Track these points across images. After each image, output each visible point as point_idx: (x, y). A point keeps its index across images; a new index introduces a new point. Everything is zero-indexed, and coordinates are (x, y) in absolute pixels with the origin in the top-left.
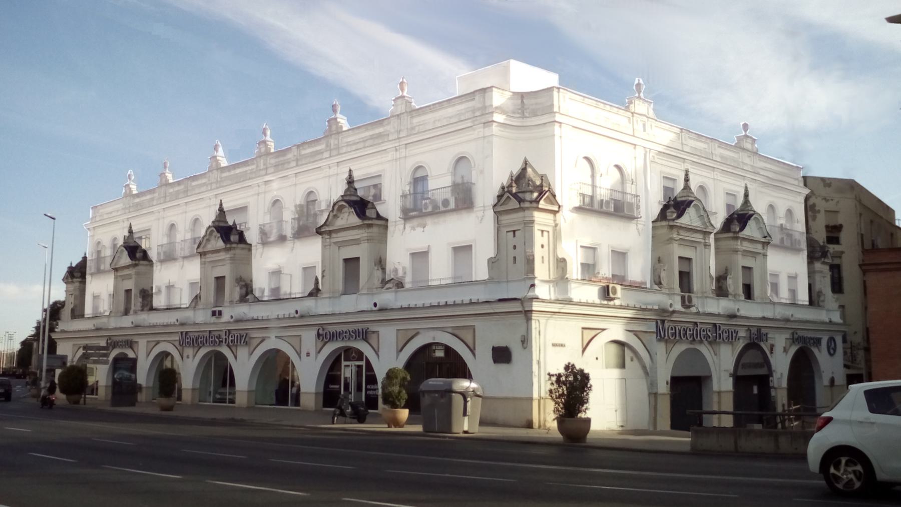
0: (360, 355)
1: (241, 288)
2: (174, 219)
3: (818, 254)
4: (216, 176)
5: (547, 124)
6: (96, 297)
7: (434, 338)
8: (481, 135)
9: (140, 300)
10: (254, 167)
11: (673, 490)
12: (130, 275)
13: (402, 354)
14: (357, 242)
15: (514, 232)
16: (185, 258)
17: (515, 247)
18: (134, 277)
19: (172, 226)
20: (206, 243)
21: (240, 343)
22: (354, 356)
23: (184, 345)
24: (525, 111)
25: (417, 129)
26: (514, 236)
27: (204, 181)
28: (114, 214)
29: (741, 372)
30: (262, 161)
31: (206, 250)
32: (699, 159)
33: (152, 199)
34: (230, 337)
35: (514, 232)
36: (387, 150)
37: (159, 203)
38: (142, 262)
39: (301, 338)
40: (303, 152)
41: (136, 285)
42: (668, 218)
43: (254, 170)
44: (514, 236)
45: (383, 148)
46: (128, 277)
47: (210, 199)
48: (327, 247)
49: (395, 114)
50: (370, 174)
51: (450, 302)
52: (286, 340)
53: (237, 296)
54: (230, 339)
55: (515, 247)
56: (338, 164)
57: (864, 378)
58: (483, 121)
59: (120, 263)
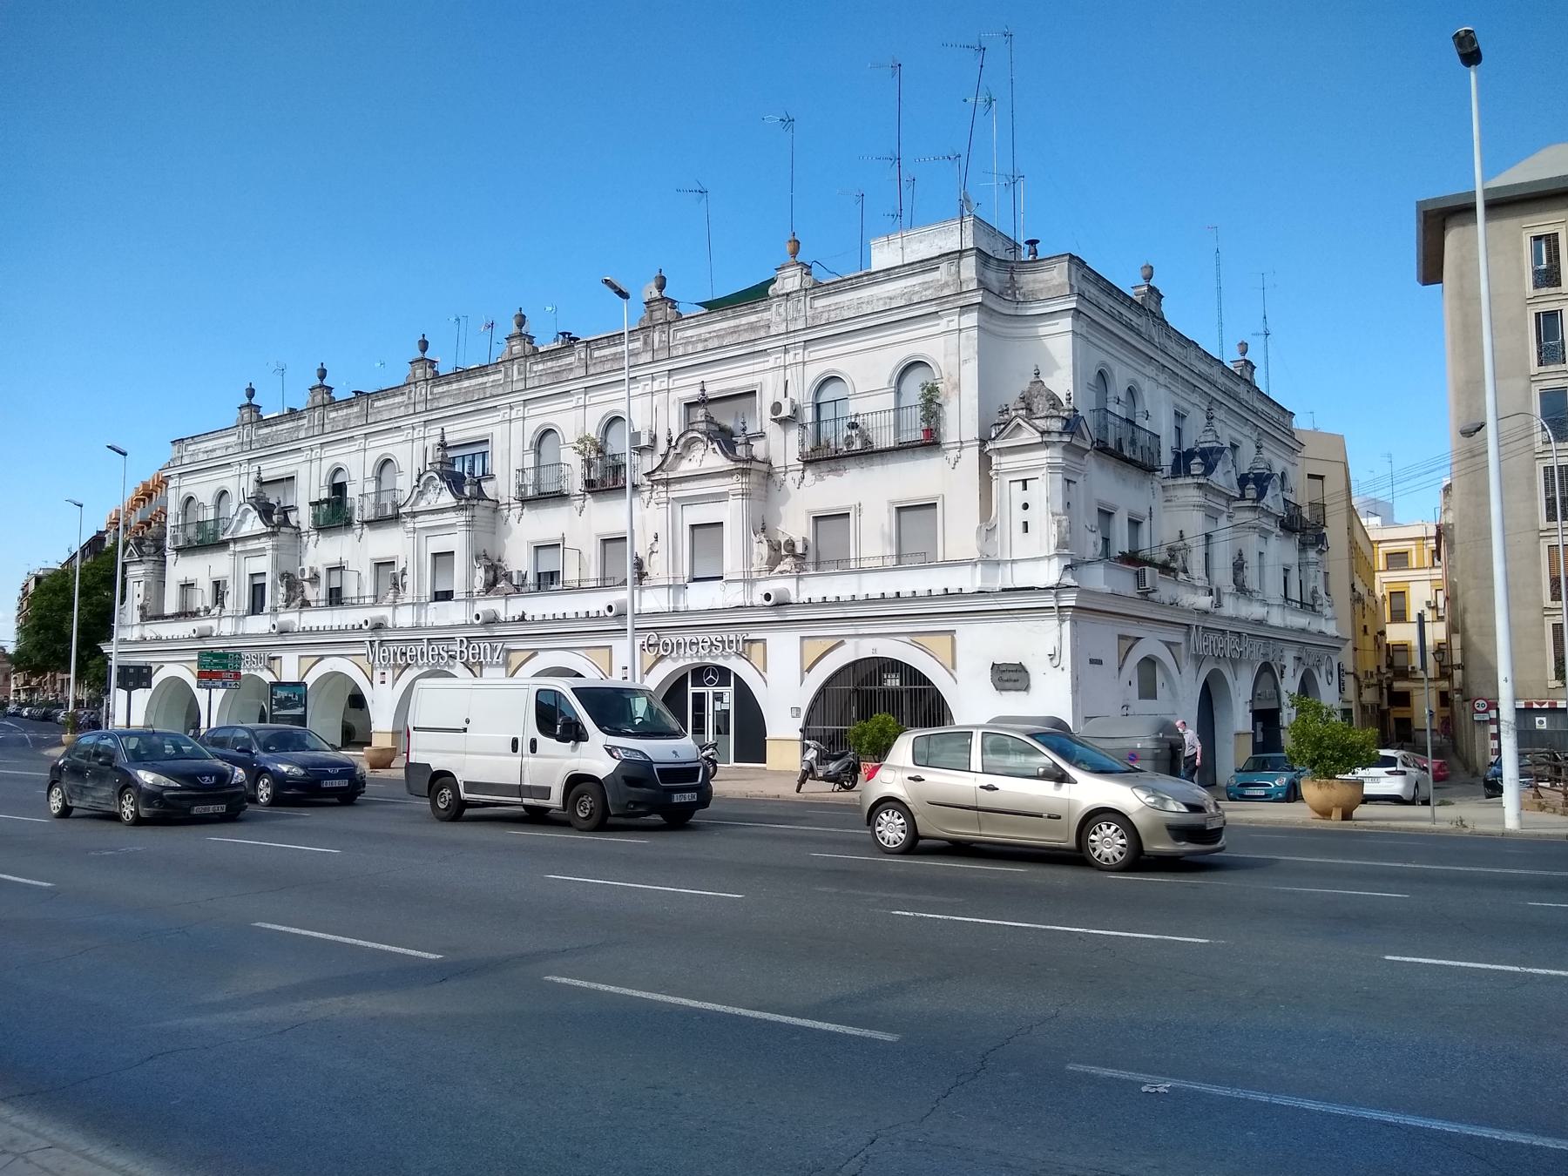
0: (723, 675)
1: (486, 572)
2: (342, 461)
3: (1311, 539)
4: (583, 356)
5: (1059, 314)
6: (187, 586)
7: (875, 650)
8: (954, 325)
9: (283, 590)
10: (500, 376)
11: (1293, 893)
12: (263, 549)
13: (809, 677)
14: (719, 498)
15: (1025, 481)
16: (371, 523)
17: (1026, 506)
18: (269, 553)
19: (385, 463)
20: (417, 498)
21: (492, 658)
22: (711, 678)
23: (377, 662)
24: (1017, 292)
25: (825, 315)
26: (1025, 488)
27: (398, 399)
28: (218, 453)
29: (1258, 707)
30: (515, 367)
31: (416, 509)
32: (1210, 389)
33: (348, 418)
34: (470, 649)
35: (1025, 481)
36: (768, 351)
37: (311, 434)
38: (283, 529)
39: (953, 641)
40: (597, 354)
41: (276, 563)
42: (1192, 473)
43: (502, 382)
44: (1025, 488)
45: (761, 348)
46: (260, 552)
47: (414, 428)
48: (660, 506)
49: (780, 293)
50: (732, 389)
51: (831, 598)
52: (582, 654)
53: (479, 584)
54: (471, 652)
55: (1026, 506)
56: (585, 391)
57: (1405, 715)
58: (961, 303)
59: (242, 531)
